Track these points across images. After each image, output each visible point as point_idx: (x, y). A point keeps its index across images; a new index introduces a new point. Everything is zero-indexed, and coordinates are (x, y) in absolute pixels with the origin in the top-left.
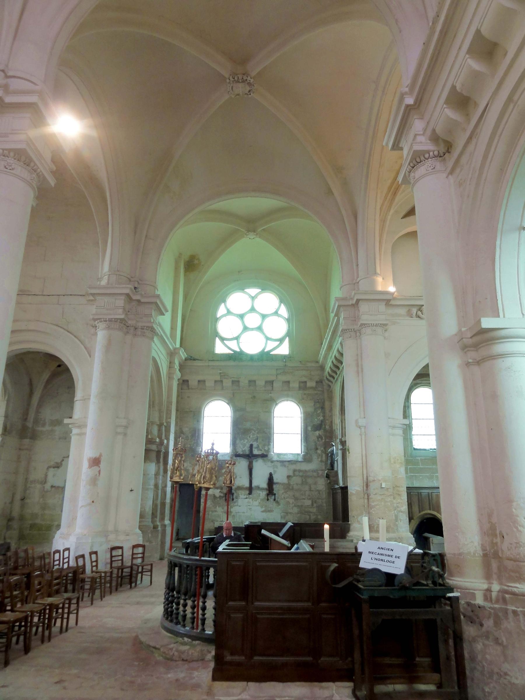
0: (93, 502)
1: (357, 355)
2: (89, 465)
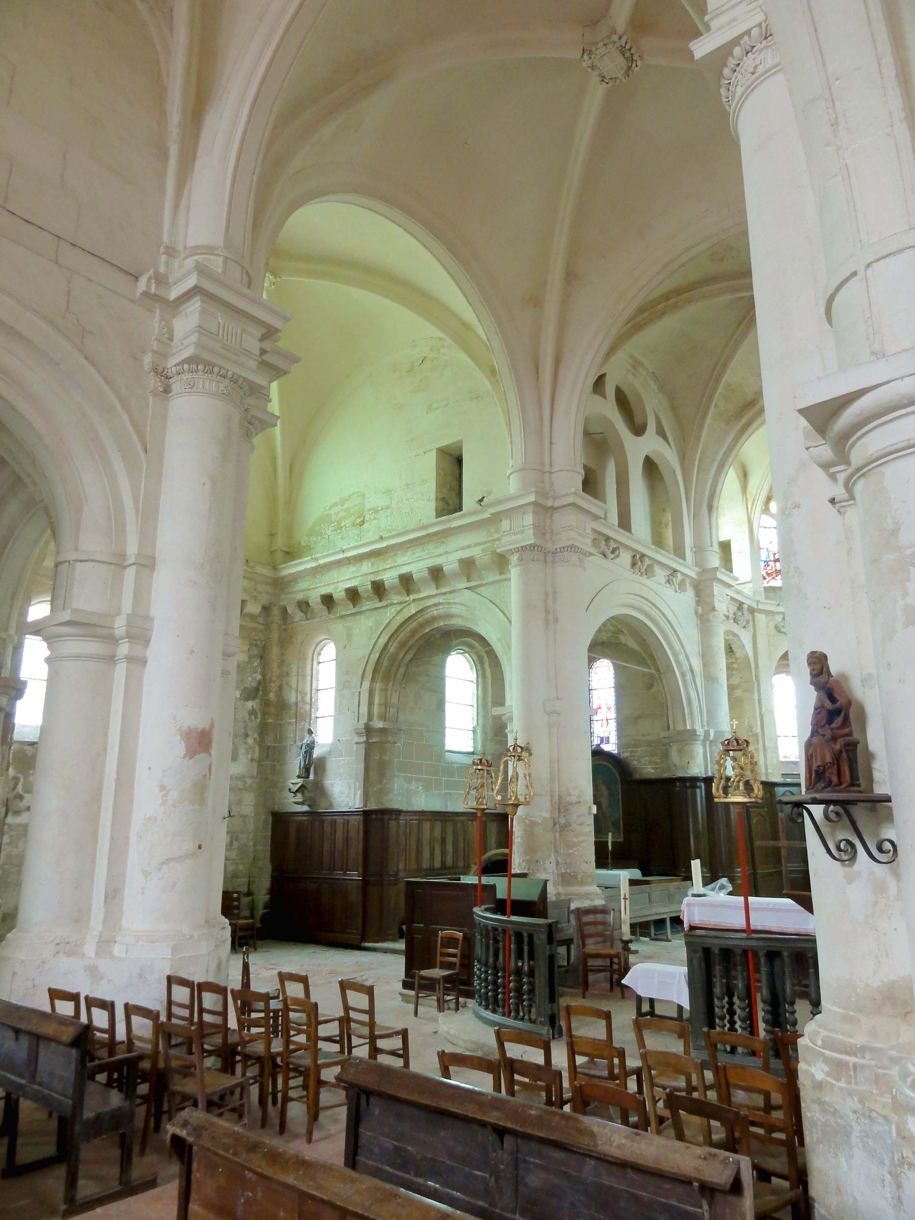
0: (200, 847)
1: (546, 593)
2: (187, 747)
